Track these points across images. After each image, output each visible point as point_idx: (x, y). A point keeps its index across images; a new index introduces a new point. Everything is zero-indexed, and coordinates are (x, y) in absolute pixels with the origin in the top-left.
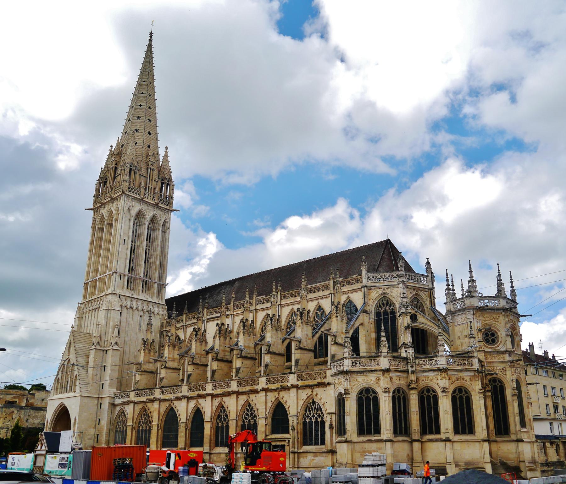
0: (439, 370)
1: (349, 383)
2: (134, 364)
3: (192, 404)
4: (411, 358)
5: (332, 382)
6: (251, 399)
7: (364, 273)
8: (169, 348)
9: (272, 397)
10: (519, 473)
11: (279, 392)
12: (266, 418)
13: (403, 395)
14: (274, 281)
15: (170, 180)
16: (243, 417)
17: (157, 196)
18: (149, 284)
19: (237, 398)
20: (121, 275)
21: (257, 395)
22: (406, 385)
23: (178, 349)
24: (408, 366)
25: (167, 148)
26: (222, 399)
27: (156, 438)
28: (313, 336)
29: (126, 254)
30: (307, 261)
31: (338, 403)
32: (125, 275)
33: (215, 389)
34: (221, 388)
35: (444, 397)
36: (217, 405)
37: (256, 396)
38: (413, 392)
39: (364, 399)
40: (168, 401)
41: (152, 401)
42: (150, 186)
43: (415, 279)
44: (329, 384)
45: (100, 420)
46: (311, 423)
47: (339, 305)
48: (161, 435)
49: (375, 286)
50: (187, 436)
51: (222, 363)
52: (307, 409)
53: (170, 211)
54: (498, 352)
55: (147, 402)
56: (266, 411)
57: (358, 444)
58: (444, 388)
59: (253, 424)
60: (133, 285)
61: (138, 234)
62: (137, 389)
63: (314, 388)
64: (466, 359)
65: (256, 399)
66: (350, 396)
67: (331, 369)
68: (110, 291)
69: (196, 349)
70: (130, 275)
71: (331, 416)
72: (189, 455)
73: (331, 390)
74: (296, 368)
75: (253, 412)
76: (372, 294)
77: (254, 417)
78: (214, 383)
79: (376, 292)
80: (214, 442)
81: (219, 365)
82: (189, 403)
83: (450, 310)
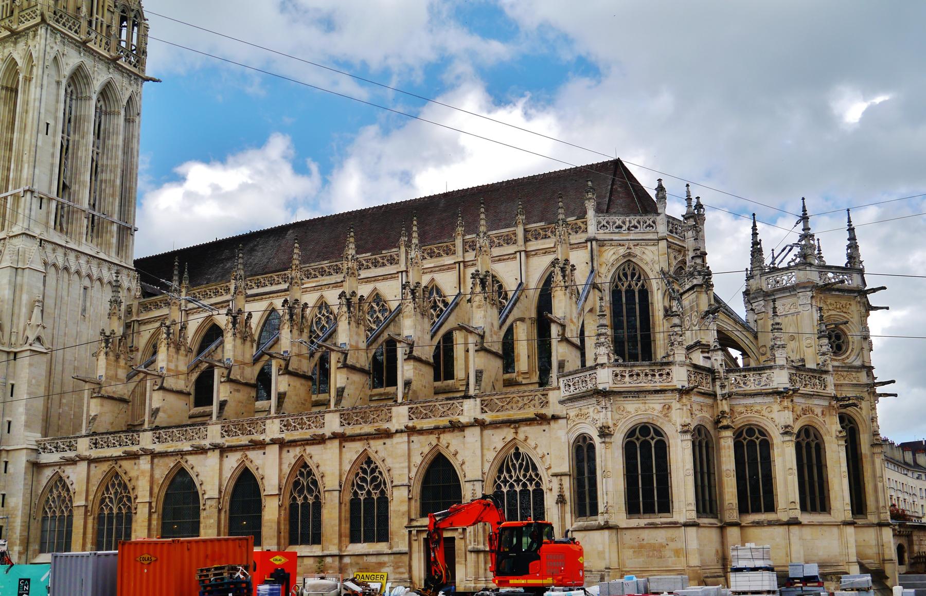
0: (776, 393)
1: (609, 413)
2: (86, 382)
3: (232, 461)
4: (721, 371)
5: (563, 414)
6: (374, 448)
7: (591, 213)
8: (168, 350)
9: (422, 446)
10: (884, 580)
11: (439, 434)
12: (409, 486)
14: (415, 218)
15: (139, 14)
16: (353, 485)
17: (113, 43)
18: (98, 224)
19: (341, 447)
20: (41, 199)
21: (388, 441)
22: (711, 421)
23: (184, 353)
24: (714, 386)
26: (305, 450)
27: (146, 531)
28: (500, 327)
29: (53, 155)
30: (446, 195)
31: (574, 454)
32: (50, 199)
33: (288, 430)
34: (302, 428)
35: (788, 443)
36: (293, 462)
37: (384, 444)
38: (728, 433)
39: (638, 445)
40: (172, 455)
41: (134, 456)
44: (555, 418)
45: (6, 497)
46: (512, 494)
47: (567, 266)
48: (157, 524)
49: (612, 240)
50: (222, 525)
51: (295, 379)
52: (503, 467)
53: (140, 80)
54: (850, 367)
55: (122, 459)
56: (409, 472)
57: (628, 532)
58: (786, 427)
59: (378, 498)
60: (68, 223)
61: (76, 117)
62: (95, 434)
63: (519, 427)
64: (818, 375)
65: (385, 449)
66: (612, 440)
67: (559, 388)
68: (16, 230)
69: (234, 351)
70: (60, 200)
71: (561, 480)
72: (272, 560)
73: (561, 429)
74: (478, 387)
75: (377, 474)
76: (605, 254)
77: (379, 484)
78: (286, 419)
79: (612, 252)
80: (287, 535)
81: (292, 384)
82: (225, 459)
83: (761, 289)
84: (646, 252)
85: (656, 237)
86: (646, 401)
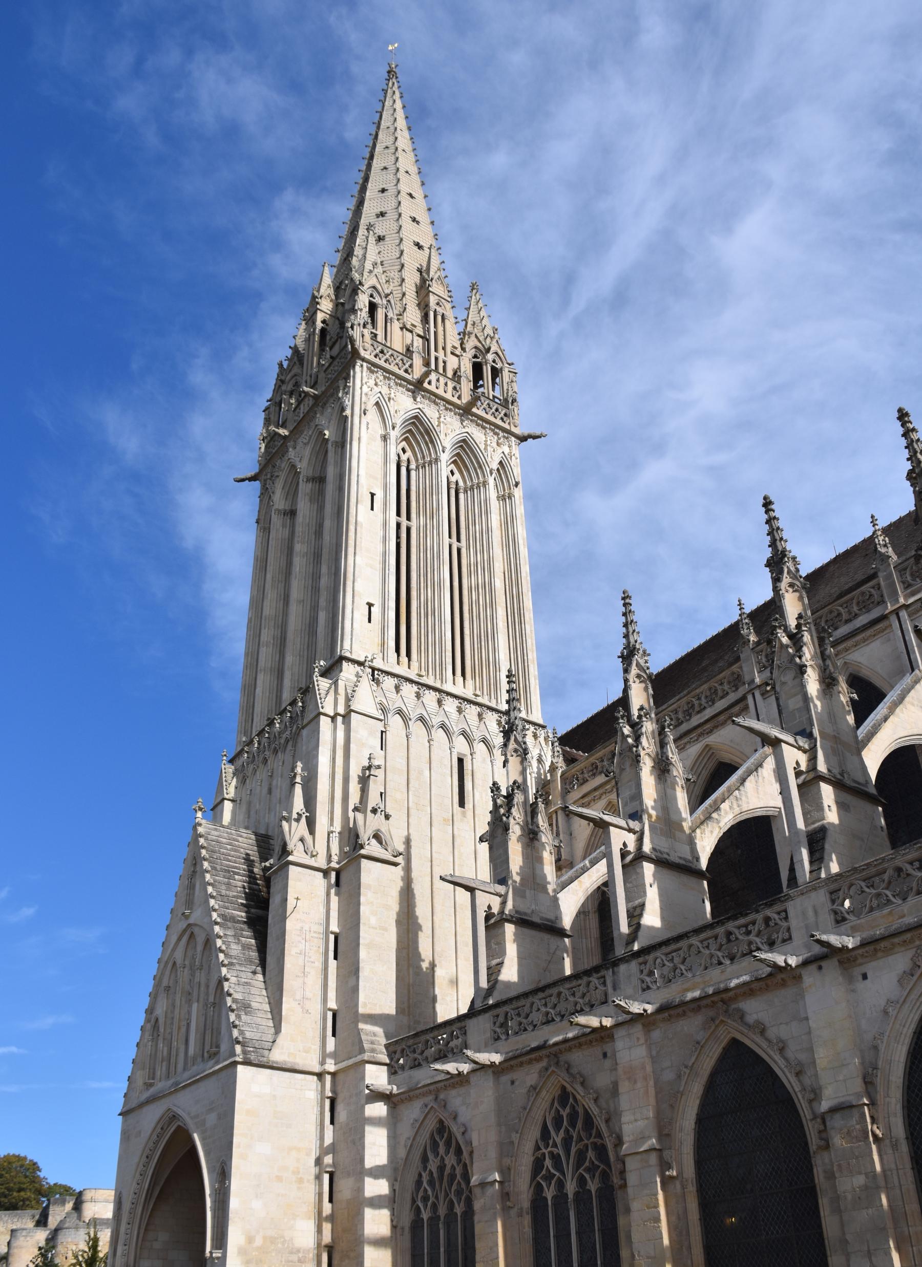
53: (513, 439)
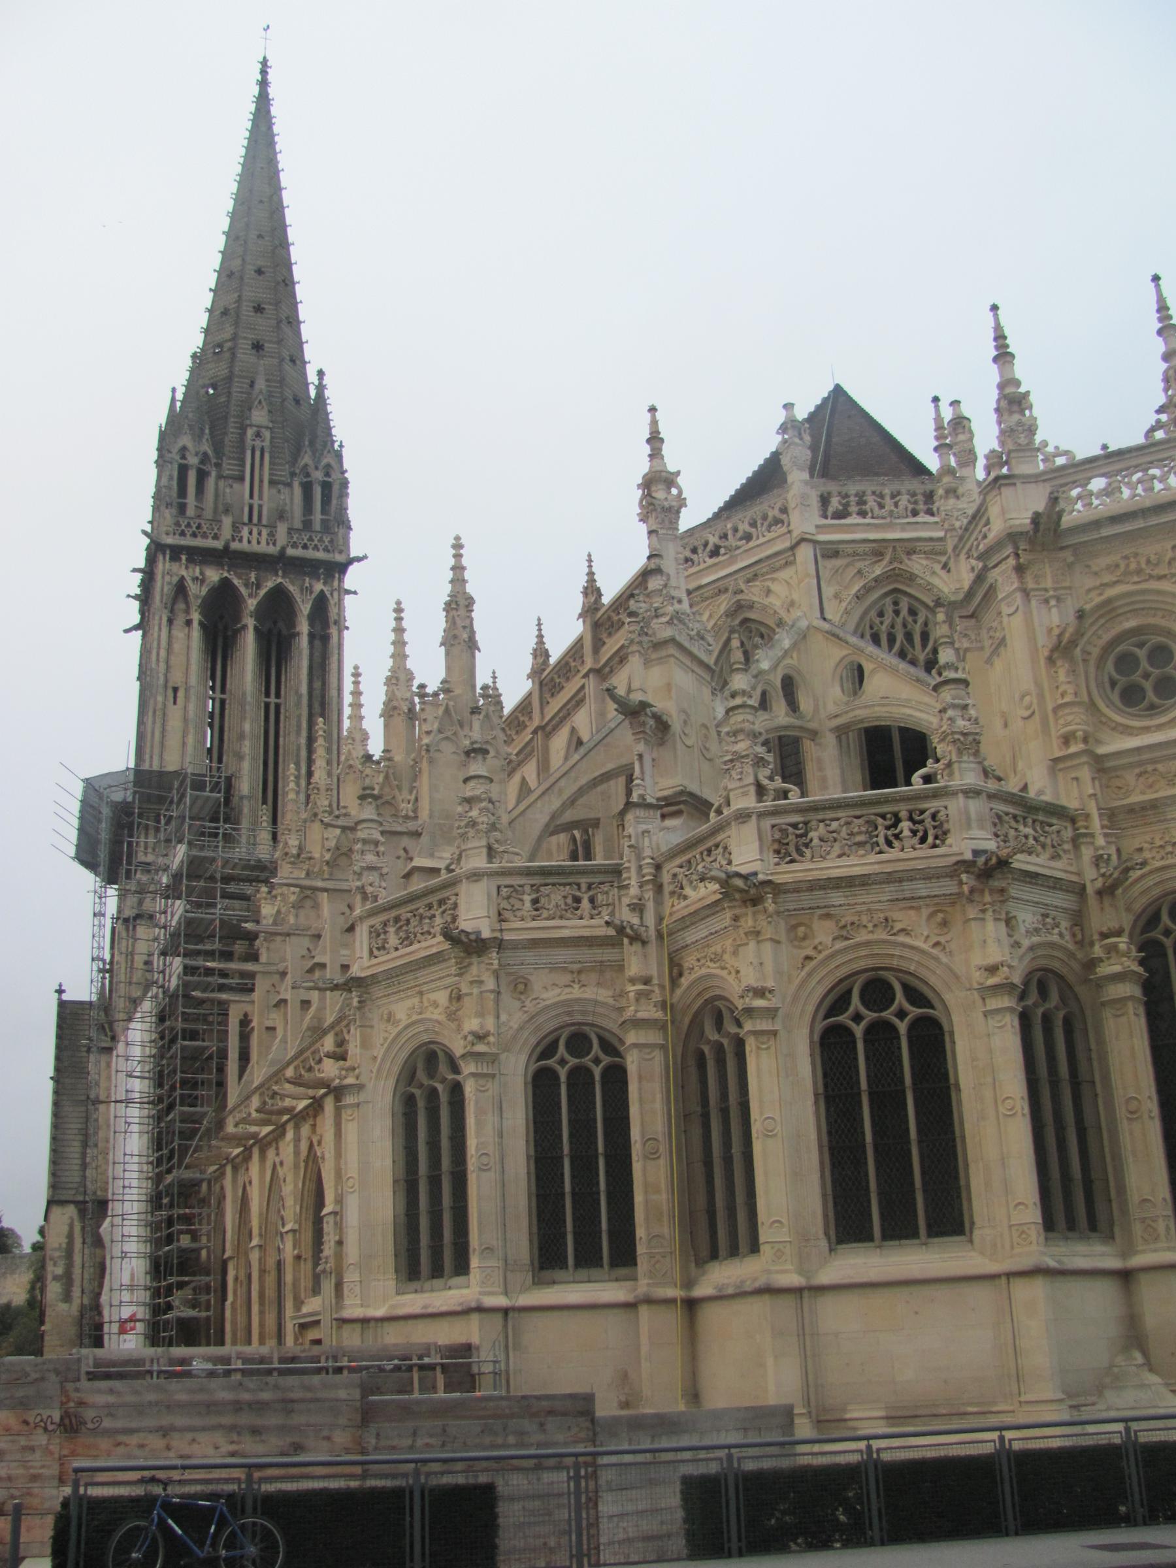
13: (606, 1060)
25: (321, 374)
42: (256, 502)
43: (881, 506)
49: (699, 588)
84: (774, 587)
85: (787, 544)
86: (425, 988)
